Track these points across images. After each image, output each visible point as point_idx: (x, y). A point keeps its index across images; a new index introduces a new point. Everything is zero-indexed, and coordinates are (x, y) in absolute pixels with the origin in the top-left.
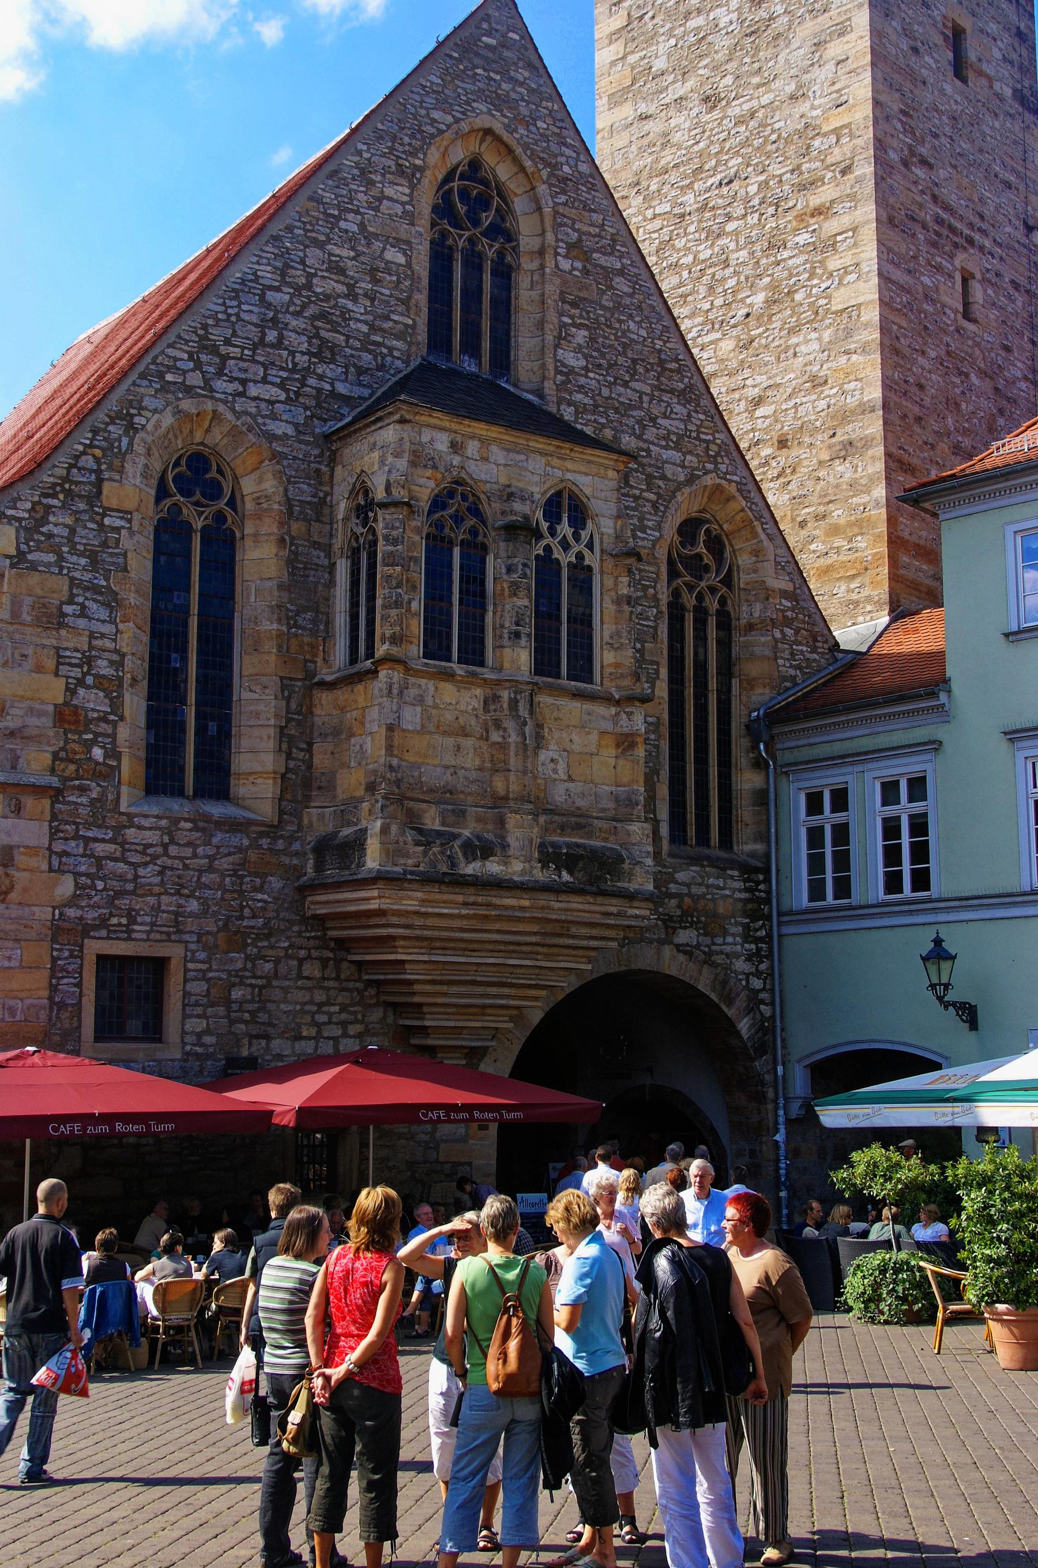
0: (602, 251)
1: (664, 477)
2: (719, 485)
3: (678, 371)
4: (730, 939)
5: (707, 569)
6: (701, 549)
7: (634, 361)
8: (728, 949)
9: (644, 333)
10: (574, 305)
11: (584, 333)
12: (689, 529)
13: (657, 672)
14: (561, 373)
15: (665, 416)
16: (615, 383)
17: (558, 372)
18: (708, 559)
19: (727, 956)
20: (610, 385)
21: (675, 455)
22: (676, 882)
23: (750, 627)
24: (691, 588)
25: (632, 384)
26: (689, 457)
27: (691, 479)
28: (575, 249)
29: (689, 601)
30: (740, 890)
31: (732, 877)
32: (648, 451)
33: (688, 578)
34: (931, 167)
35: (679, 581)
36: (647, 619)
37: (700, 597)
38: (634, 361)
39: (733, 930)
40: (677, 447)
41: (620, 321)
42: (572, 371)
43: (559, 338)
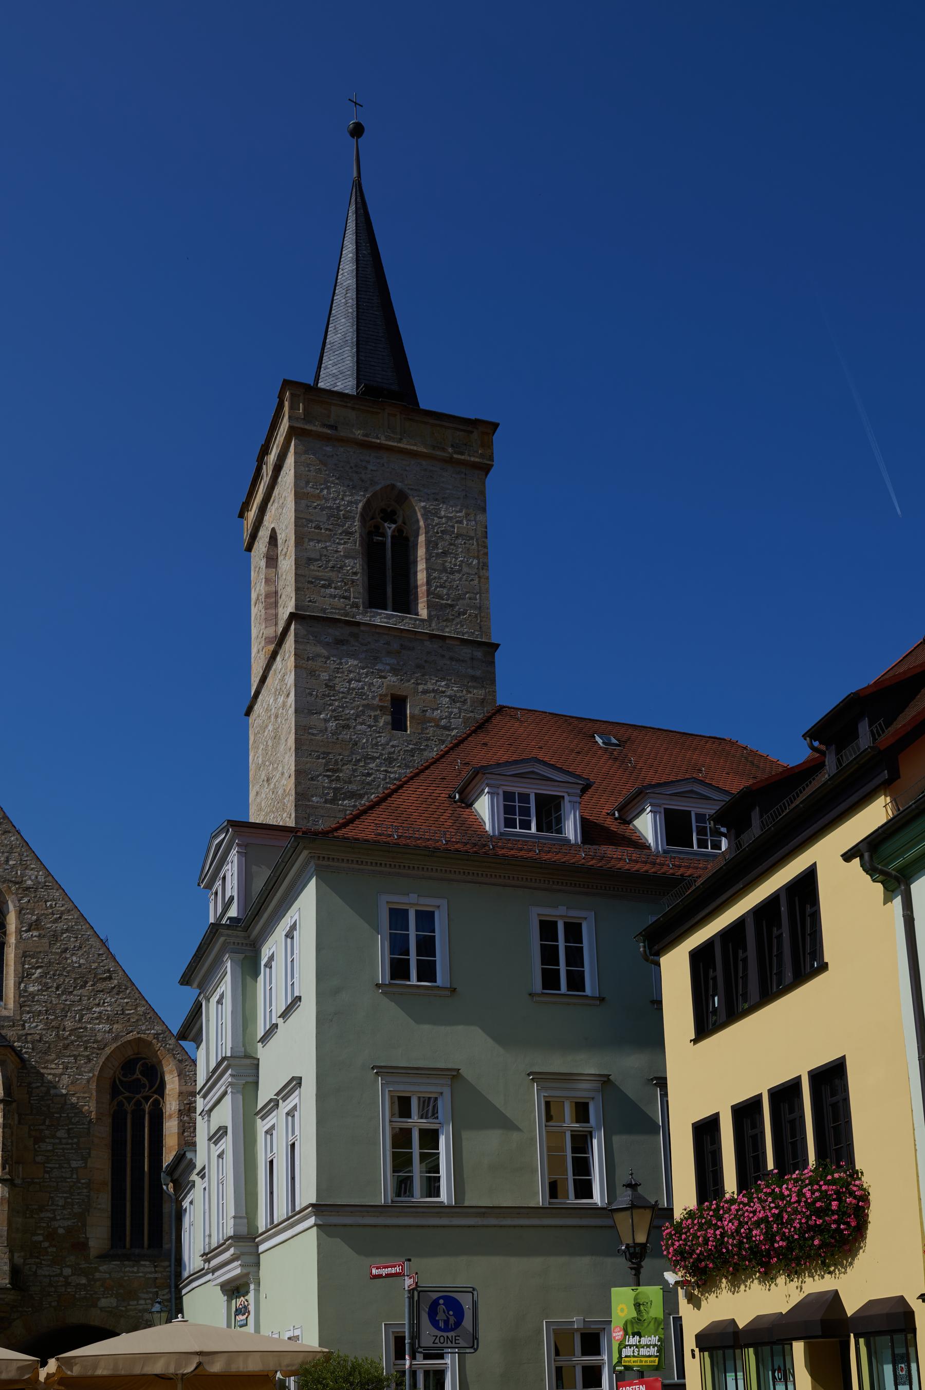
0: (56, 921)
1: (96, 1041)
2: (139, 1038)
3: (110, 978)
4: (142, 1302)
5: (144, 1086)
6: (137, 1075)
7: (75, 979)
8: (141, 1307)
9: (82, 961)
10: (32, 957)
11: (39, 971)
12: (128, 1066)
13: (89, 1154)
14: (23, 996)
15: (98, 1005)
16: (63, 993)
17: (20, 996)
18: (144, 1080)
19: (140, 1311)
20: (59, 996)
21: (107, 1027)
22: (100, 1272)
23: (170, 1116)
24: (129, 1099)
25: (75, 993)
26: (115, 1026)
27: (115, 1039)
28: (35, 925)
29: (129, 1107)
30: (151, 1273)
31: (144, 1266)
32: (86, 1028)
33: (127, 1094)
34: (361, 797)
35: (120, 1098)
36: (83, 1124)
37: (138, 1104)
38: (75, 979)
39: (146, 1296)
40: (110, 1020)
41: (66, 959)
42: (33, 995)
43: (23, 978)
